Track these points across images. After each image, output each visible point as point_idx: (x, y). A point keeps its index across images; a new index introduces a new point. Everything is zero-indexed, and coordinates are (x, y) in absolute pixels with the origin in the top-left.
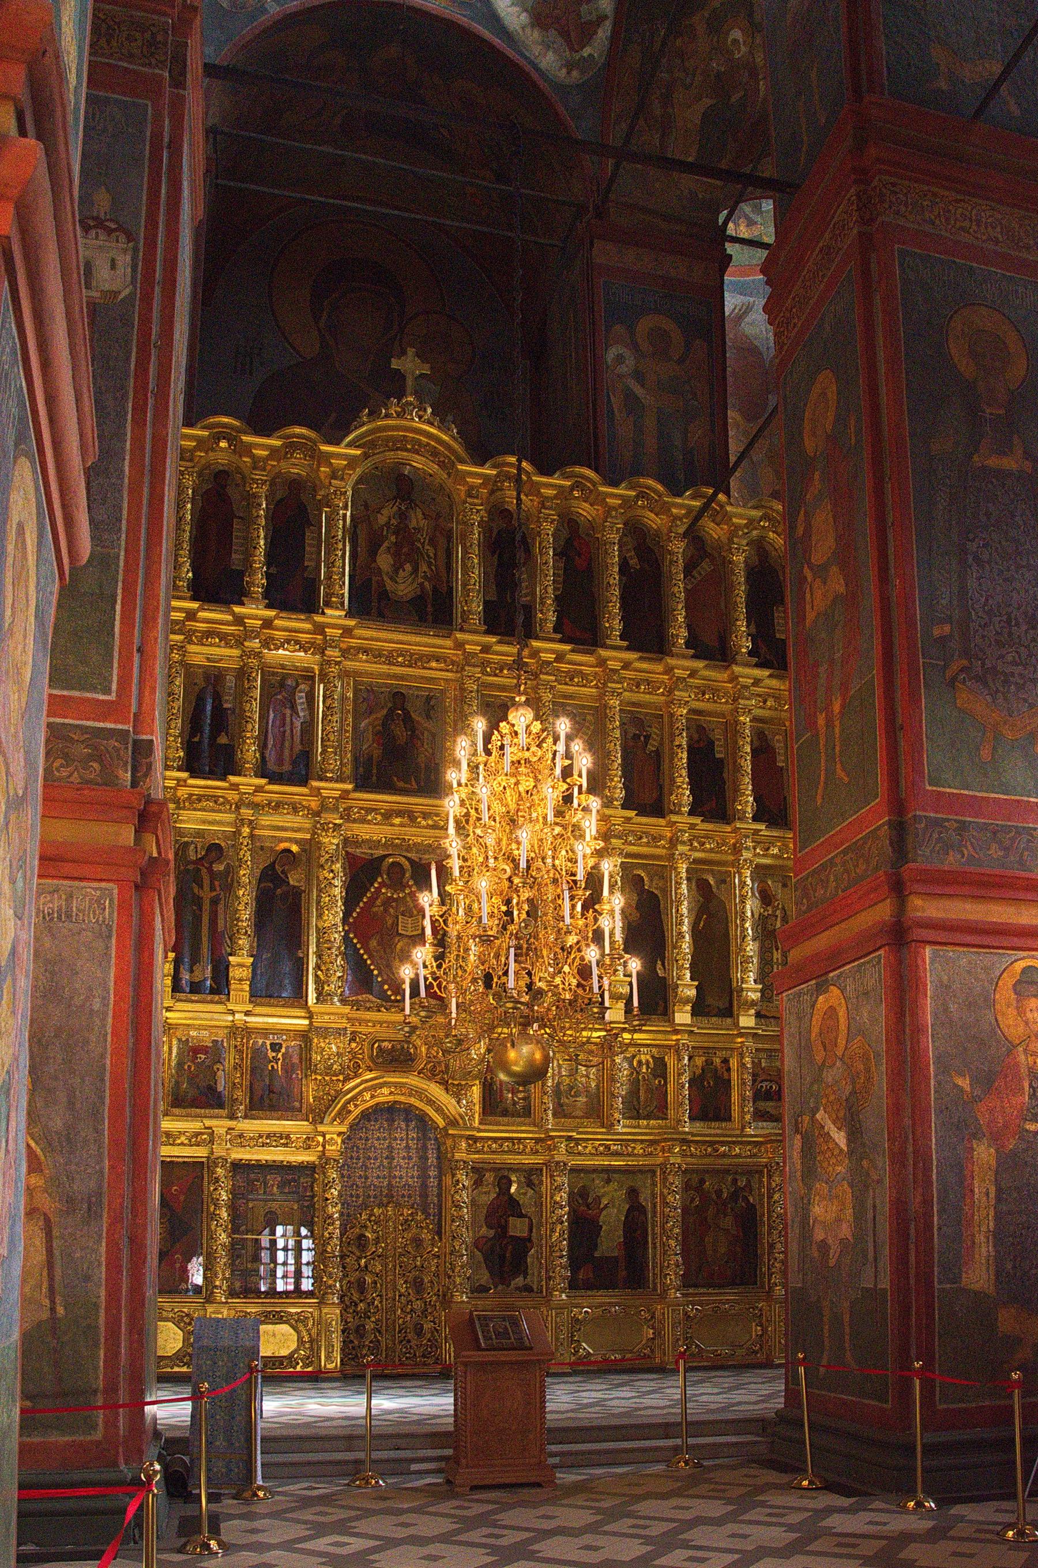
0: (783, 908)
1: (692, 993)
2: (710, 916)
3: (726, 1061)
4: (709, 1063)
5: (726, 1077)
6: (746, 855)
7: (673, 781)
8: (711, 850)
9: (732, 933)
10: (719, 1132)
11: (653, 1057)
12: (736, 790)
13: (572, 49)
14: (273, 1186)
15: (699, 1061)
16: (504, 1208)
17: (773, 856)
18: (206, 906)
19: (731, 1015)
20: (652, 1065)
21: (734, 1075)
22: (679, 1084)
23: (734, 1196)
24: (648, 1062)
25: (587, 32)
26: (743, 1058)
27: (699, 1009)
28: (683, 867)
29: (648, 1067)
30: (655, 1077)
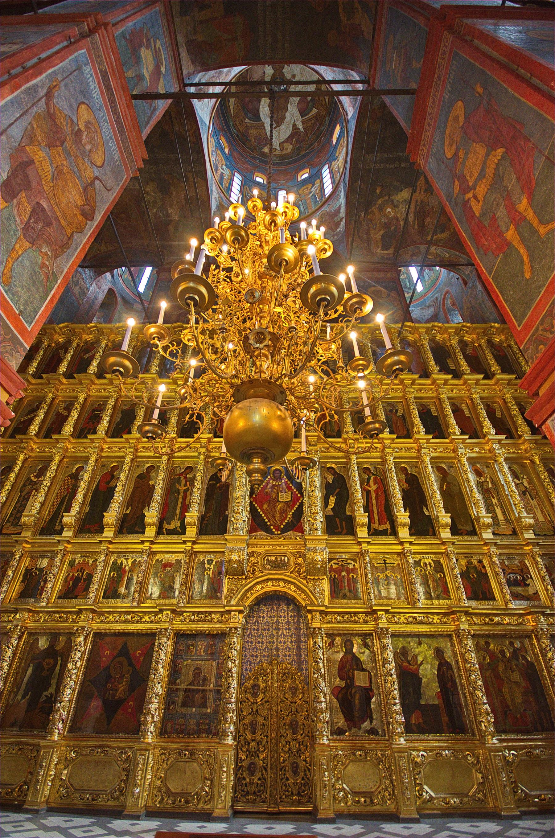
0: (490, 478)
1: (448, 520)
2: (448, 483)
3: (480, 562)
4: (469, 563)
5: (483, 571)
6: (460, 451)
7: (413, 423)
8: (441, 452)
9: (464, 491)
10: (488, 607)
11: (432, 560)
12: (448, 426)
13: (333, 231)
14: (201, 649)
15: (463, 562)
16: (349, 666)
17: (476, 452)
18: (181, 494)
19: (476, 534)
20: (433, 565)
21: (488, 569)
22: (453, 575)
23: (516, 653)
24: (430, 564)
25: (338, 224)
26: (491, 558)
27: (455, 531)
28: (427, 460)
29: (431, 567)
30: (437, 572)
